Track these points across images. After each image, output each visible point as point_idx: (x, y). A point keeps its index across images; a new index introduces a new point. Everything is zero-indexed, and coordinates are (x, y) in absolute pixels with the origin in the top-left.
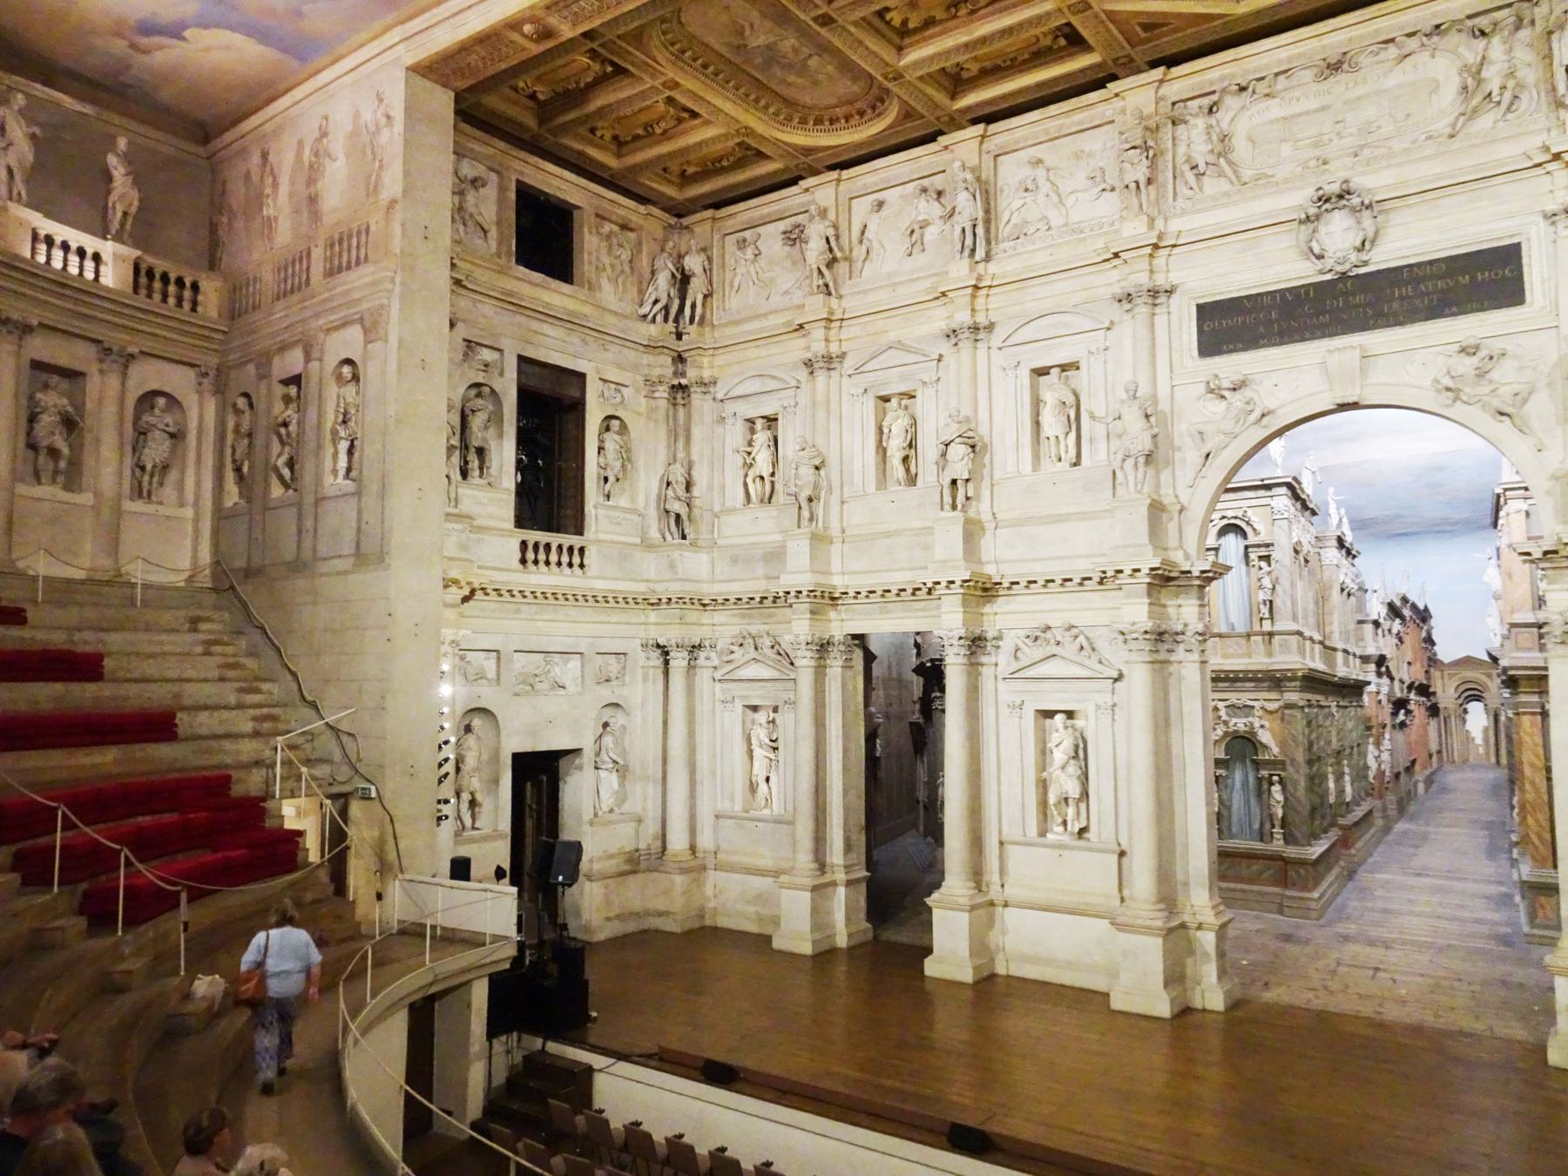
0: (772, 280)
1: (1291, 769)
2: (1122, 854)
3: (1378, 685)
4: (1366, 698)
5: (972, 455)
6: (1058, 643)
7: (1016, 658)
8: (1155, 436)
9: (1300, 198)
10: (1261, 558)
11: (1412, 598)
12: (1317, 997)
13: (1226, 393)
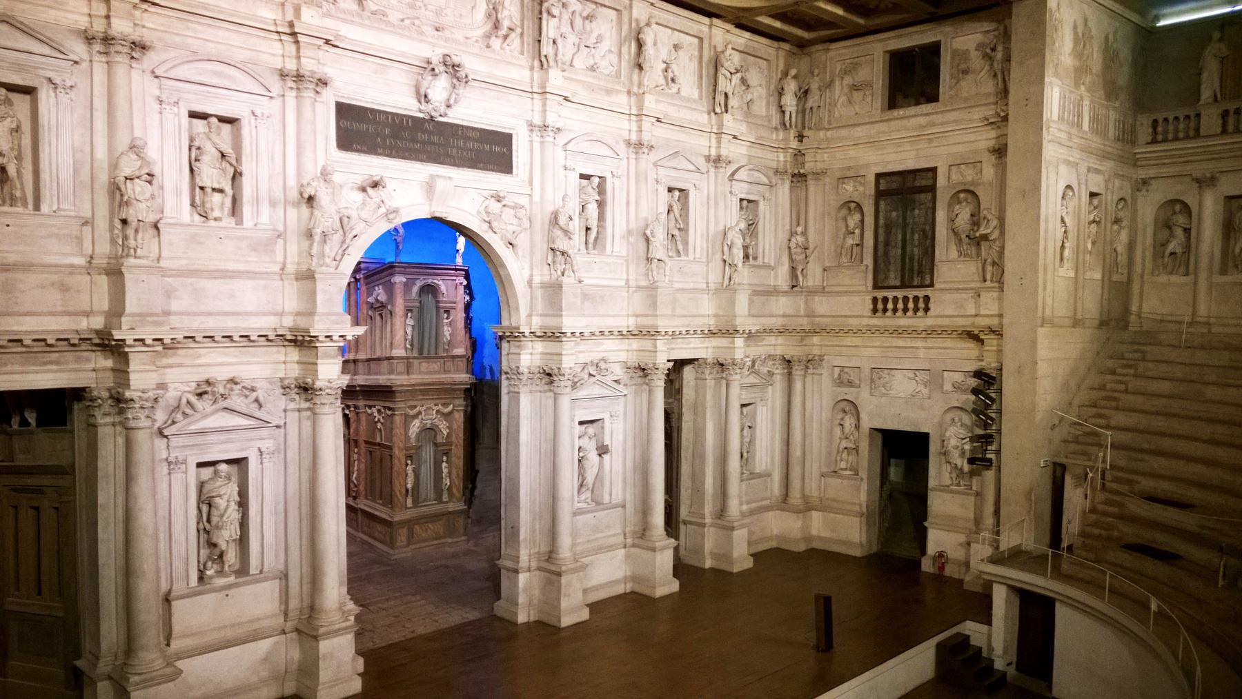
7: (185, 415)
9: (436, 57)
13: (369, 189)
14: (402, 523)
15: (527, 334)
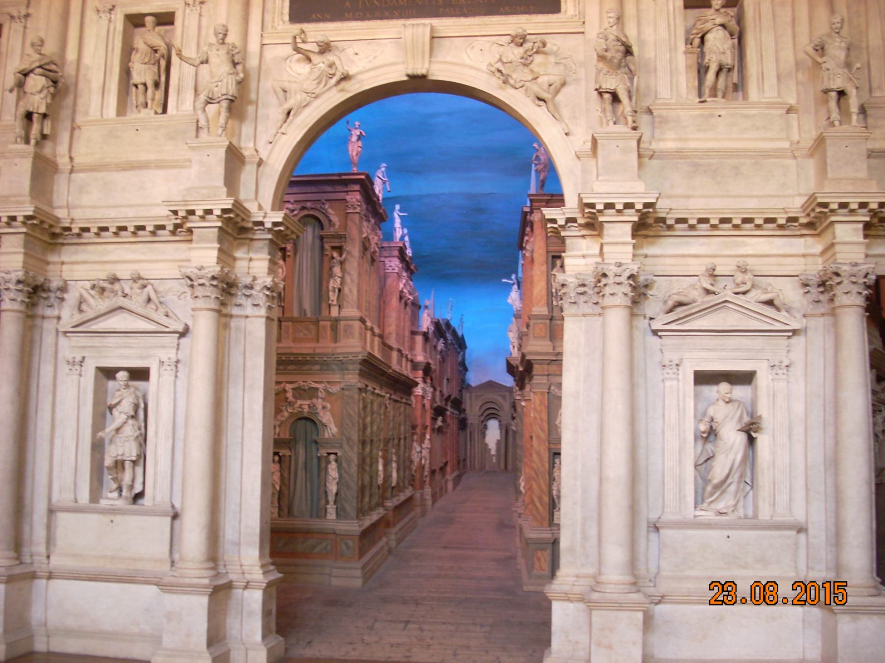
1: (346, 447)
2: (175, 516)
3: (424, 389)
4: (412, 398)
5: (52, 90)
6: (125, 296)
7: (81, 311)
8: (239, 83)
10: (333, 248)
11: (454, 324)
12: (354, 649)
14: (540, 544)
15: (561, 222)
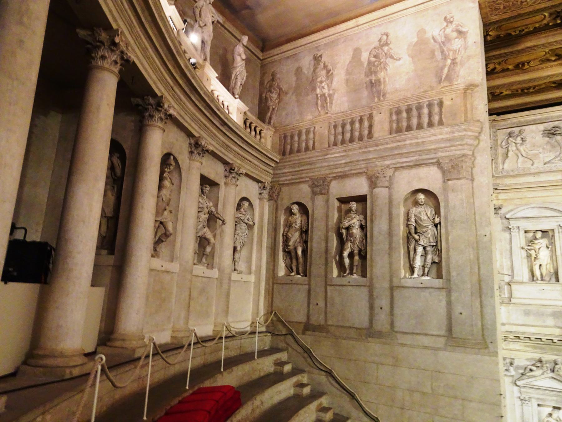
0: (536, 155)
